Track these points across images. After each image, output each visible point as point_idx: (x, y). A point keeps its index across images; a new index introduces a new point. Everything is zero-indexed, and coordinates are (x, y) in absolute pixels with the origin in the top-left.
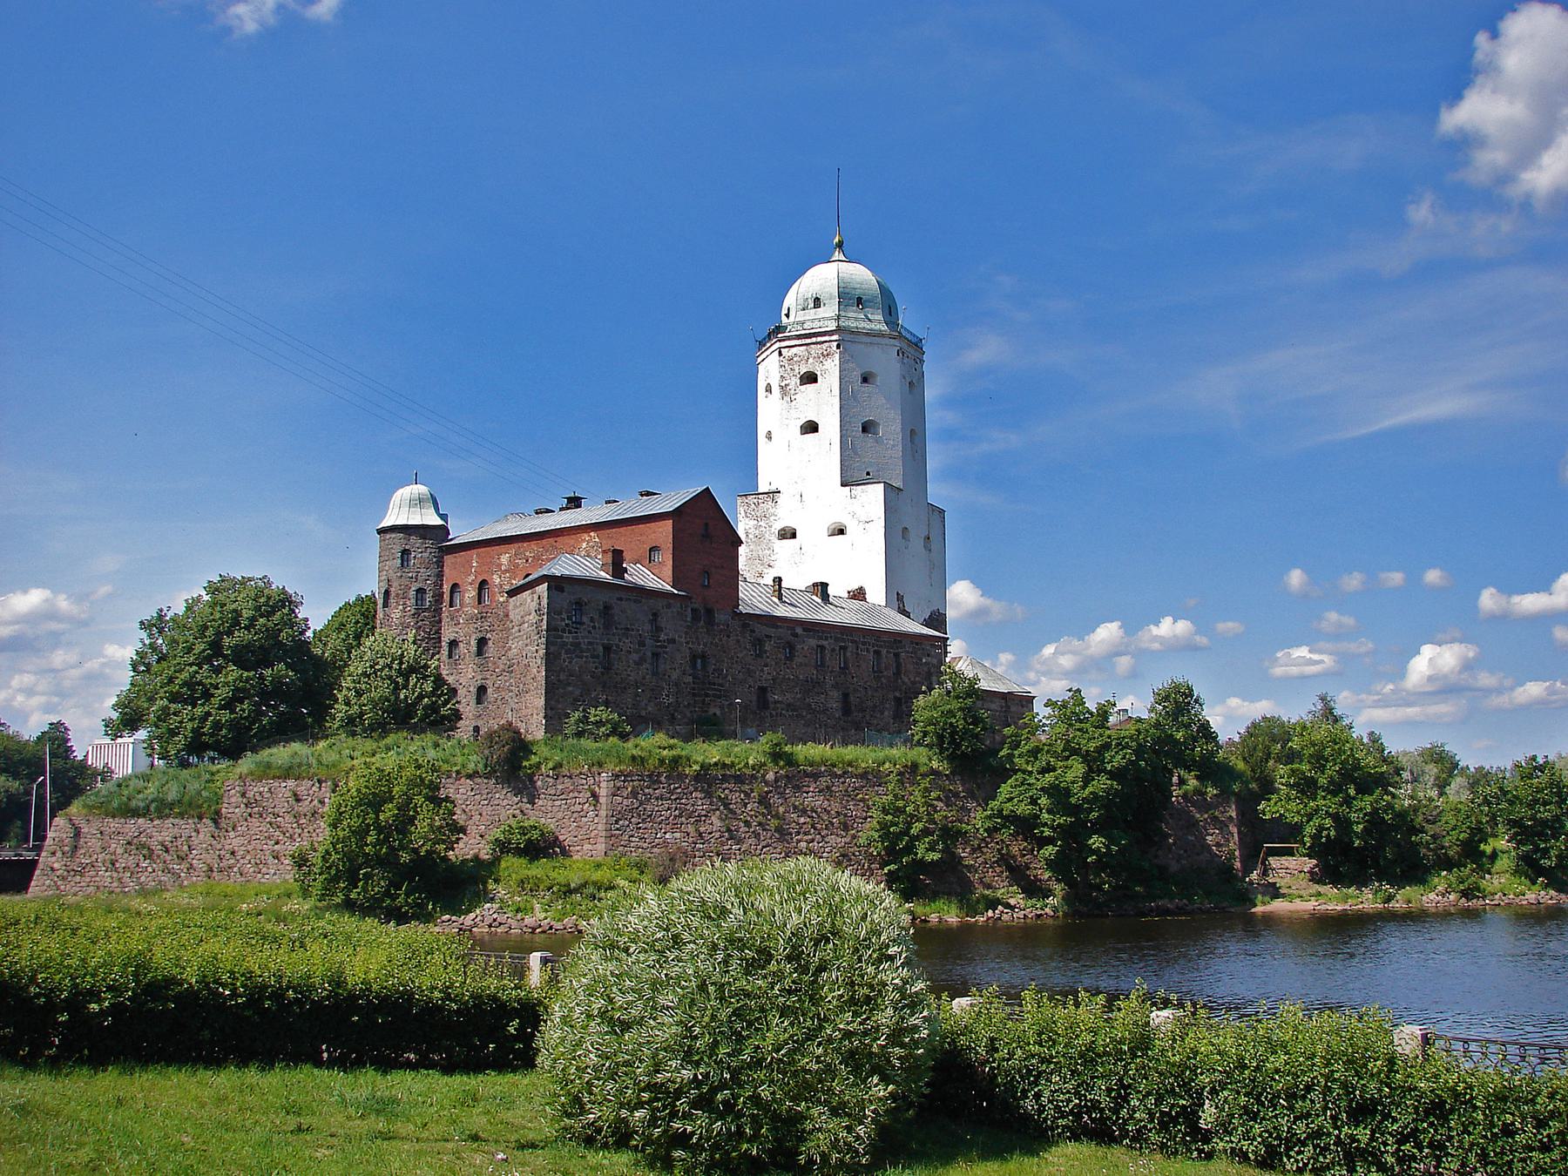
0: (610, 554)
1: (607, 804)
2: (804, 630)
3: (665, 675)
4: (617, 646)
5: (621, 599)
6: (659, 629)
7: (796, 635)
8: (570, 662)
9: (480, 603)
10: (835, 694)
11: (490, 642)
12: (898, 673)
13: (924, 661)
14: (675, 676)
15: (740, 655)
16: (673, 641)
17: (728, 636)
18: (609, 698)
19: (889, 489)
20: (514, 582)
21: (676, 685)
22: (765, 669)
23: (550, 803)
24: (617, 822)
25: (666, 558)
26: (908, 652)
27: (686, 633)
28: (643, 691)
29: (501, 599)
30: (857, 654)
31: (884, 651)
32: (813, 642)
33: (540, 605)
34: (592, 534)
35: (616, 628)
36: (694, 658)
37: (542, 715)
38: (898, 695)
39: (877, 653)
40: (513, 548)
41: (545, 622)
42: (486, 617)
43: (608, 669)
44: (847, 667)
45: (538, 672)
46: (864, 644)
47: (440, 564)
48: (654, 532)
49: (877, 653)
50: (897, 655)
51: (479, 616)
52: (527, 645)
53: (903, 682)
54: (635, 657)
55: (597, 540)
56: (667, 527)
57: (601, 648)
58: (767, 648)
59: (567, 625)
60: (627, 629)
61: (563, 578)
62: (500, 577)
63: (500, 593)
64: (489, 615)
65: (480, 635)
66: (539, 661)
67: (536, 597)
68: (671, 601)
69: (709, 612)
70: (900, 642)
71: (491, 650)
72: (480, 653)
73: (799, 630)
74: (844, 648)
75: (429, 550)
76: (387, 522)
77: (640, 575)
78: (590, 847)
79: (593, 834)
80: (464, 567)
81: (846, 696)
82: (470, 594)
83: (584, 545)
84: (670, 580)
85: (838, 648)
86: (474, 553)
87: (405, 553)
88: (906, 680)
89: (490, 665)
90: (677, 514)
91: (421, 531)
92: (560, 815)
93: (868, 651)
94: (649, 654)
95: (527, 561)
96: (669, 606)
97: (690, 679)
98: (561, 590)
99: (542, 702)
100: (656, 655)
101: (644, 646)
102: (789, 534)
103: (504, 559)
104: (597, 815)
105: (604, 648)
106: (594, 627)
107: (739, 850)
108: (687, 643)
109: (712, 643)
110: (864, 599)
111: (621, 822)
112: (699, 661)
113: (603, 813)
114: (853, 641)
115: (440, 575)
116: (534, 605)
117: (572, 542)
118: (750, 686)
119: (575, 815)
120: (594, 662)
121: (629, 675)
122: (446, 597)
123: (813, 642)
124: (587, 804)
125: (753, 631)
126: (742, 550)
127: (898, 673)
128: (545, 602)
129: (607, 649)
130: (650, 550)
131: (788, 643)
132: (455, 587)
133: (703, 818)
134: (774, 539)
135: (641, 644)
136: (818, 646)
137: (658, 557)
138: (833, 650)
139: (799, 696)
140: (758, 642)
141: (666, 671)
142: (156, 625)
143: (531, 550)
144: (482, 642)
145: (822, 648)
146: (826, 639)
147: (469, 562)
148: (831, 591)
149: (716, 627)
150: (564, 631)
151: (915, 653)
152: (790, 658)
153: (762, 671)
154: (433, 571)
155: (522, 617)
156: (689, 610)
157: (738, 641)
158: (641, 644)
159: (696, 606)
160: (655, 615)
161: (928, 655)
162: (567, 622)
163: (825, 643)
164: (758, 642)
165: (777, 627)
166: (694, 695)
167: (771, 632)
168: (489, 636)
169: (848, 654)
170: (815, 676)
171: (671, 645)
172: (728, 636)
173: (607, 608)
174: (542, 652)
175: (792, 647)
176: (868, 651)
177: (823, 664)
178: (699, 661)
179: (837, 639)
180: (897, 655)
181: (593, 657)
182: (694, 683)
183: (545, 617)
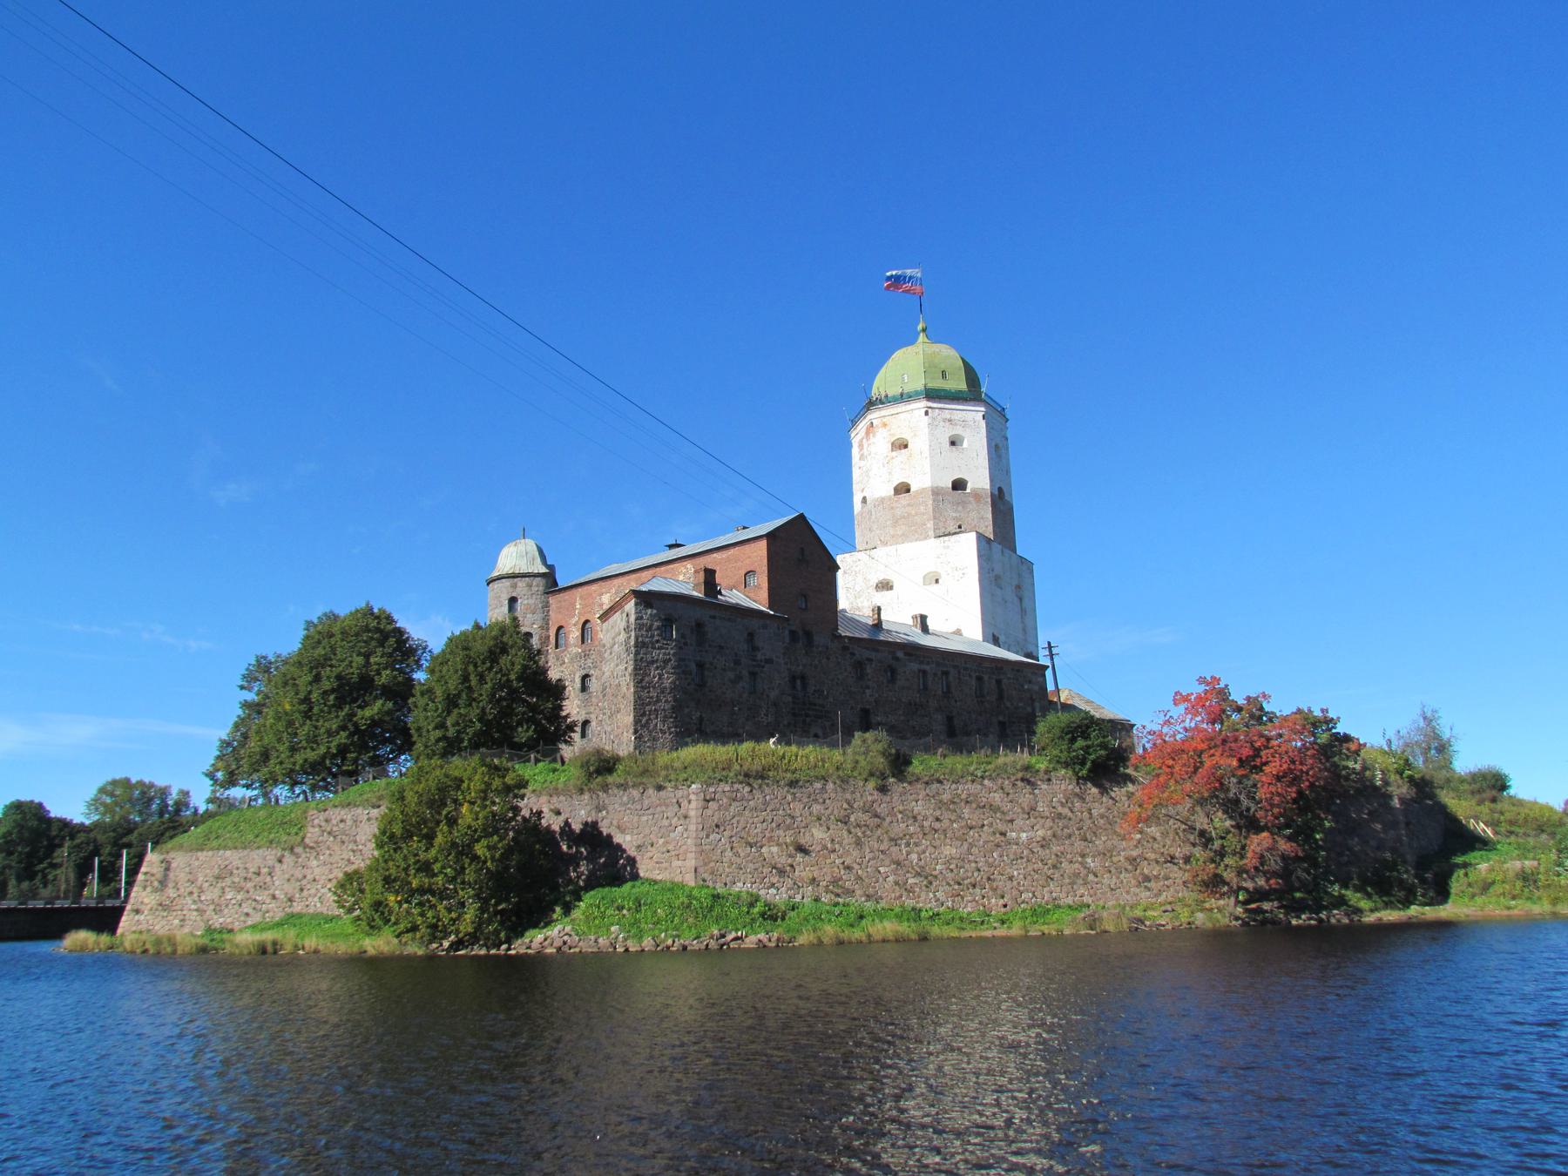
0: (702, 574)
1: (697, 817)
2: (906, 654)
3: (762, 694)
4: (711, 664)
5: (714, 617)
6: (755, 649)
7: (897, 659)
8: (660, 678)
9: (583, 642)
10: (939, 717)
11: (593, 679)
12: (1001, 697)
13: (1026, 687)
14: (773, 694)
15: (840, 677)
16: (769, 661)
17: (828, 659)
18: (704, 715)
19: (980, 537)
21: (775, 705)
22: (867, 691)
23: (636, 818)
24: (708, 836)
25: (762, 581)
26: (1009, 678)
27: (784, 654)
28: (740, 709)
30: (959, 679)
31: (986, 677)
32: (915, 666)
34: (689, 566)
35: (710, 646)
36: (793, 679)
37: (632, 731)
38: (1001, 718)
39: (979, 679)
41: (633, 638)
43: (702, 685)
44: (949, 691)
45: (627, 688)
46: (966, 669)
47: (546, 605)
48: (749, 557)
49: (979, 679)
50: (999, 682)
52: (617, 665)
53: (1007, 708)
54: (731, 675)
56: (763, 544)
57: (693, 666)
58: (869, 670)
59: (658, 641)
60: (721, 647)
61: (651, 594)
65: (584, 672)
66: (628, 678)
67: (625, 615)
68: (768, 622)
69: (808, 635)
70: (1002, 668)
71: (594, 685)
72: (584, 688)
73: (900, 654)
74: (946, 673)
75: (534, 597)
76: (496, 574)
77: (733, 596)
78: (680, 863)
79: (682, 850)
80: (568, 610)
81: (950, 719)
82: (574, 634)
84: (766, 601)
85: (940, 673)
88: (1008, 704)
90: (771, 537)
92: (647, 832)
93: (970, 676)
94: (745, 673)
96: (765, 627)
97: (790, 699)
98: (648, 605)
99: (631, 718)
100: (753, 674)
101: (740, 664)
102: (885, 586)
104: (686, 830)
105: (697, 665)
106: (685, 644)
107: (843, 863)
108: (786, 664)
109: (811, 665)
110: (961, 635)
111: (711, 837)
112: (798, 682)
113: (692, 827)
114: (955, 667)
115: (546, 620)
116: (623, 624)
118: (852, 708)
119: (662, 830)
120: (686, 679)
121: (724, 693)
122: (553, 640)
123: (915, 666)
124: (676, 819)
125: (853, 654)
126: (839, 574)
127: (1001, 697)
128: (632, 618)
129: (700, 666)
130: (746, 575)
131: (889, 666)
132: (560, 628)
133: (803, 830)
134: (872, 591)
135: (737, 662)
136: (920, 671)
137: (753, 581)
138: (935, 674)
139: (902, 718)
140: (859, 666)
141: (764, 690)
142: (262, 668)
144: (585, 677)
145: (924, 672)
146: (928, 663)
147: (573, 605)
148: (929, 622)
149: (814, 649)
150: (654, 648)
151: (1017, 680)
152: (893, 680)
153: (864, 693)
154: (539, 616)
155: (613, 639)
156: (787, 632)
157: (839, 663)
158: (737, 662)
159: (793, 628)
160: (751, 635)
161: (1030, 682)
162: (656, 638)
163: (927, 668)
164: (859, 666)
165: (877, 651)
166: (794, 715)
167: (873, 655)
168: (592, 672)
169: (951, 679)
170: (918, 700)
171: (767, 666)
172: (828, 659)
173: (699, 625)
174: (630, 668)
175: (893, 671)
176: (970, 676)
177: (925, 688)
178: (798, 682)
179: (938, 664)
180: (999, 682)
181: (684, 673)
182: (794, 703)
183: (633, 634)
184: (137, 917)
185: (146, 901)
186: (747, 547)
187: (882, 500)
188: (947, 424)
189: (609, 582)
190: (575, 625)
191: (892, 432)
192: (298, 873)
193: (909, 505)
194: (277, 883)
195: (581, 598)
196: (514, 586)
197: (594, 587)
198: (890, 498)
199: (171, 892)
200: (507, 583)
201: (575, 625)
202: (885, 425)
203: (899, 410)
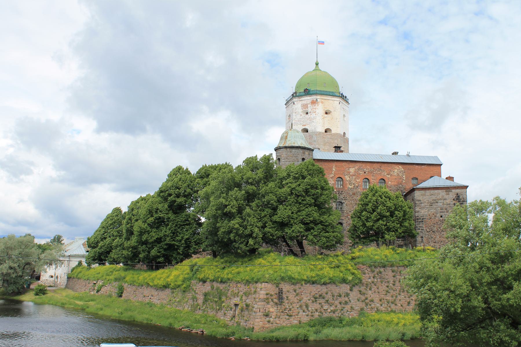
20: (358, 180)
29: (350, 187)
33: (459, 197)
34: (400, 167)
40: (357, 166)
42: (341, 193)
48: (432, 171)
51: (337, 192)
55: (402, 169)
62: (350, 177)
63: (350, 184)
64: (343, 192)
83: (396, 171)
86: (334, 165)
87: (303, 159)
89: (345, 214)
91: (308, 151)
95: (365, 172)
103: (352, 170)
117: (389, 168)
143: (367, 168)
184: (268, 319)
185: (271, 310)
186: (432, 168)
187: (320, 133)
188: (343, 109)
189: (353, 164)
190: (332, 178)
191: (325, 107)
192: (363, 298)
193: (331, 138)
194: (352, 301)
195: (336, 166)
196: (304, 153)
197: (344, 164)
198: (323, 133)
199: (286, 305)
200: (301, 151)
201: (332, 178)
202: (322, 102)
203: (329, 98)
